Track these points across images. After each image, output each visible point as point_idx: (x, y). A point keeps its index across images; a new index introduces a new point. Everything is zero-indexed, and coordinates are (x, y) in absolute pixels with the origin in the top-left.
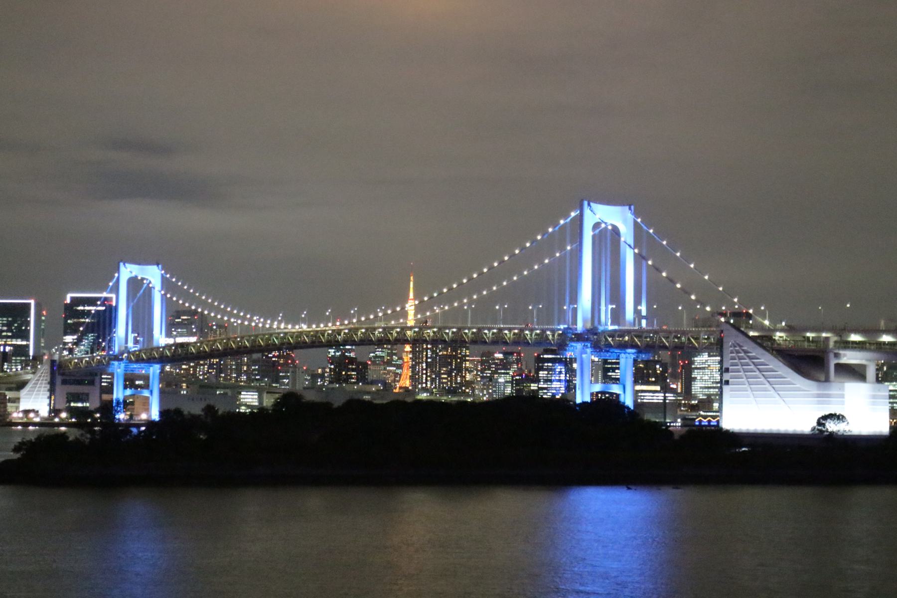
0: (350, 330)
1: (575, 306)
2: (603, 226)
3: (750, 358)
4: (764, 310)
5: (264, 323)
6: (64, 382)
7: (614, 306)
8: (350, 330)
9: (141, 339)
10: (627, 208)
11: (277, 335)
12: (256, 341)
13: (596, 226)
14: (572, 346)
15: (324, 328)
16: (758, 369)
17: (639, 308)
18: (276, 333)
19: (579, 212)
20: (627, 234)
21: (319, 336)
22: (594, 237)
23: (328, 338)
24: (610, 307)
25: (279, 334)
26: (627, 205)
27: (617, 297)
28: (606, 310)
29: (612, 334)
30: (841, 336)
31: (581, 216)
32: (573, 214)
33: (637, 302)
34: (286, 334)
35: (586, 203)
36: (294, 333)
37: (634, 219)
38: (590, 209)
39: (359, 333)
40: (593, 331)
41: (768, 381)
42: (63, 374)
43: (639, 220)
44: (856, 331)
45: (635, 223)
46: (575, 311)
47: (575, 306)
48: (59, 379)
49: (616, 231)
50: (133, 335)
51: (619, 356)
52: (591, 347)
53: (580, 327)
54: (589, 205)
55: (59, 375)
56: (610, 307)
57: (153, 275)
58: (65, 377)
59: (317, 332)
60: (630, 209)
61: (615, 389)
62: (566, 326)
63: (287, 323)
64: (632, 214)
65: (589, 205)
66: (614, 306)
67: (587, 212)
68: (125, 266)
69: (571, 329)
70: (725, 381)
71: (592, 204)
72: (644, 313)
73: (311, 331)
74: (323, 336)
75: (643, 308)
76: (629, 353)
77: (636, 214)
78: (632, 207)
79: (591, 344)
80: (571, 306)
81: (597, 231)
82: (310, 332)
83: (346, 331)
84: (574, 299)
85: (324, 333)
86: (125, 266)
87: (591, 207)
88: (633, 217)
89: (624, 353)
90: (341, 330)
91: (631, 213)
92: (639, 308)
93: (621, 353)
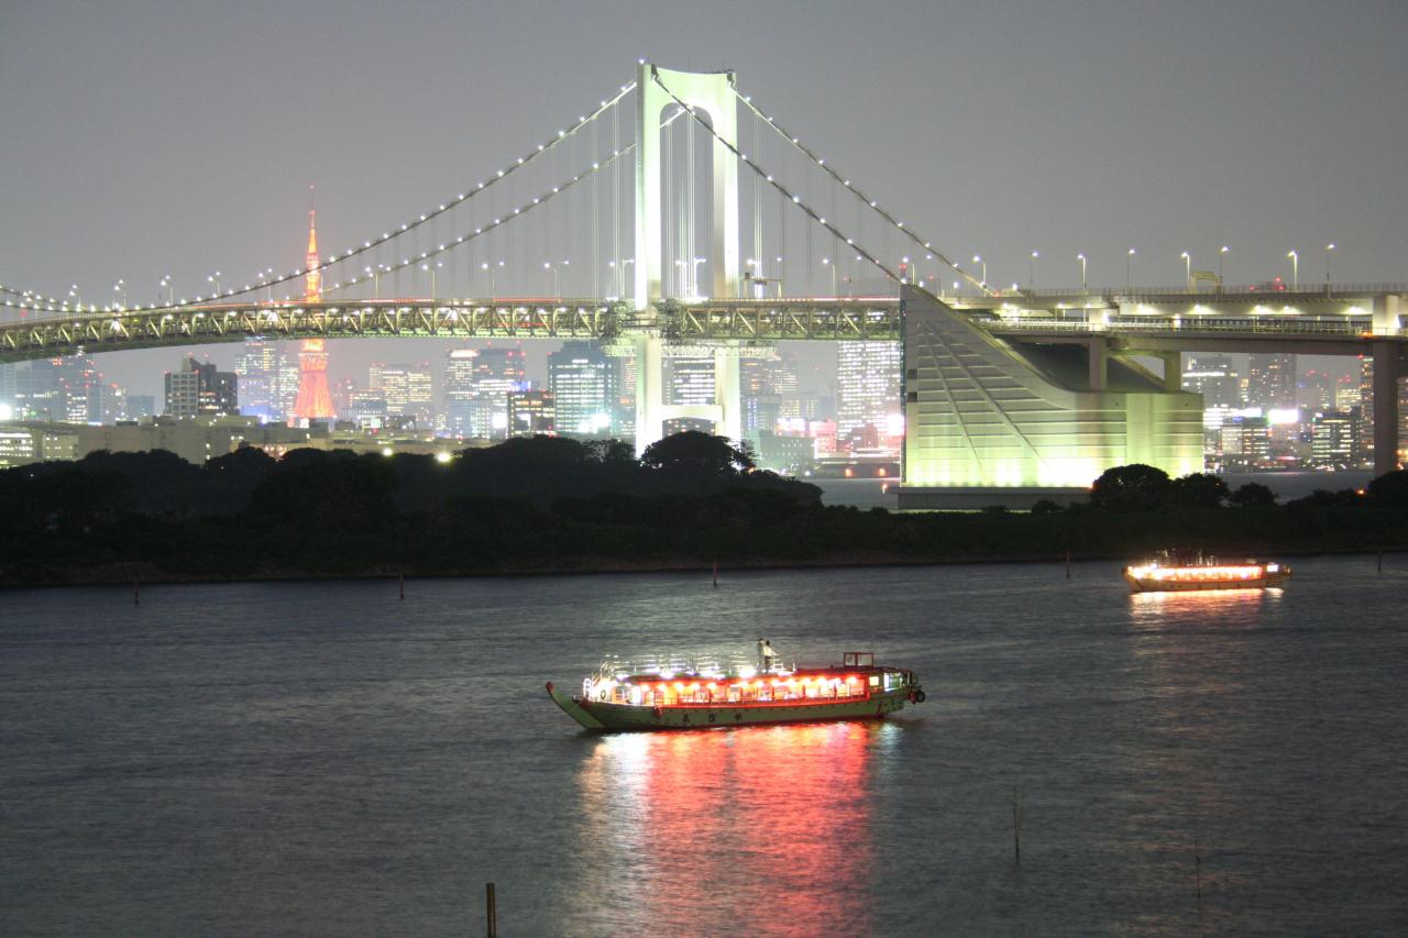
0: (208, 313)
1: (632, 261)
2: (681, 111)
3: (955, 351)
4: (979, 263)
5: (45, 301)
7: (704, 261)
8: (208, 313)
10: (725, 75)
11: (68, 325)
12: (28, 338)
13: (667, 111)
14: (627, 335)
15: (157, 311)
16: (970, 371)
17: (750, 262)
18: (66, 321)
19: (635, 85)
20: (726, 126)
21: (150, 326)
22: (663, 131)
23: (167, 329)
24: (696, 262)
25: (72, 322)
26: (725, 72)
27: (710, 246)
28: (689, 266)
29: (700, 312)
30: (1115, 306)
31: (640, 91)
32: (625, 90)
33: (746, 249)
34: (86, 322)
35: (648, 69)
36: (101, 320)
37: (737, 97)
38: (656, 79)
39: (226, 319)
41: (989, 394)
43: (747, 100)
44: (1148, 298)
45: (740, 103)
46: (630, 269)
47: (632, 261)
49: (704, 123)
51: (713, 352)
52: (661, 337)
53: (640, 302)
54: (654, 71)
56: (696, 262)
59: (145, 318)
60: (730, 78)
62: (616, 299)
63: (86, 303)
65: (654, 71)
66: (704, 261)
67: (650, 85)
69: (624, 304)
70: (910, 394)
71: (659, 70)
72: (758, 274)
73: (136, 316)
74: (158, 325)
75: (757, 264)
76: (732, 347)
77: (741, 88)
78: (734, 75)
79: (663, 331)
80: (625, 262)
81: (669, 122)
82: (130, 317)
83: (201, 315)
84: (629, 250)
85: (159, 320)
87: (657, 75)
88: (736, 93)
89: (724, 347)
90: (191, 314)
92: (750, 262)
93: (716, 347)
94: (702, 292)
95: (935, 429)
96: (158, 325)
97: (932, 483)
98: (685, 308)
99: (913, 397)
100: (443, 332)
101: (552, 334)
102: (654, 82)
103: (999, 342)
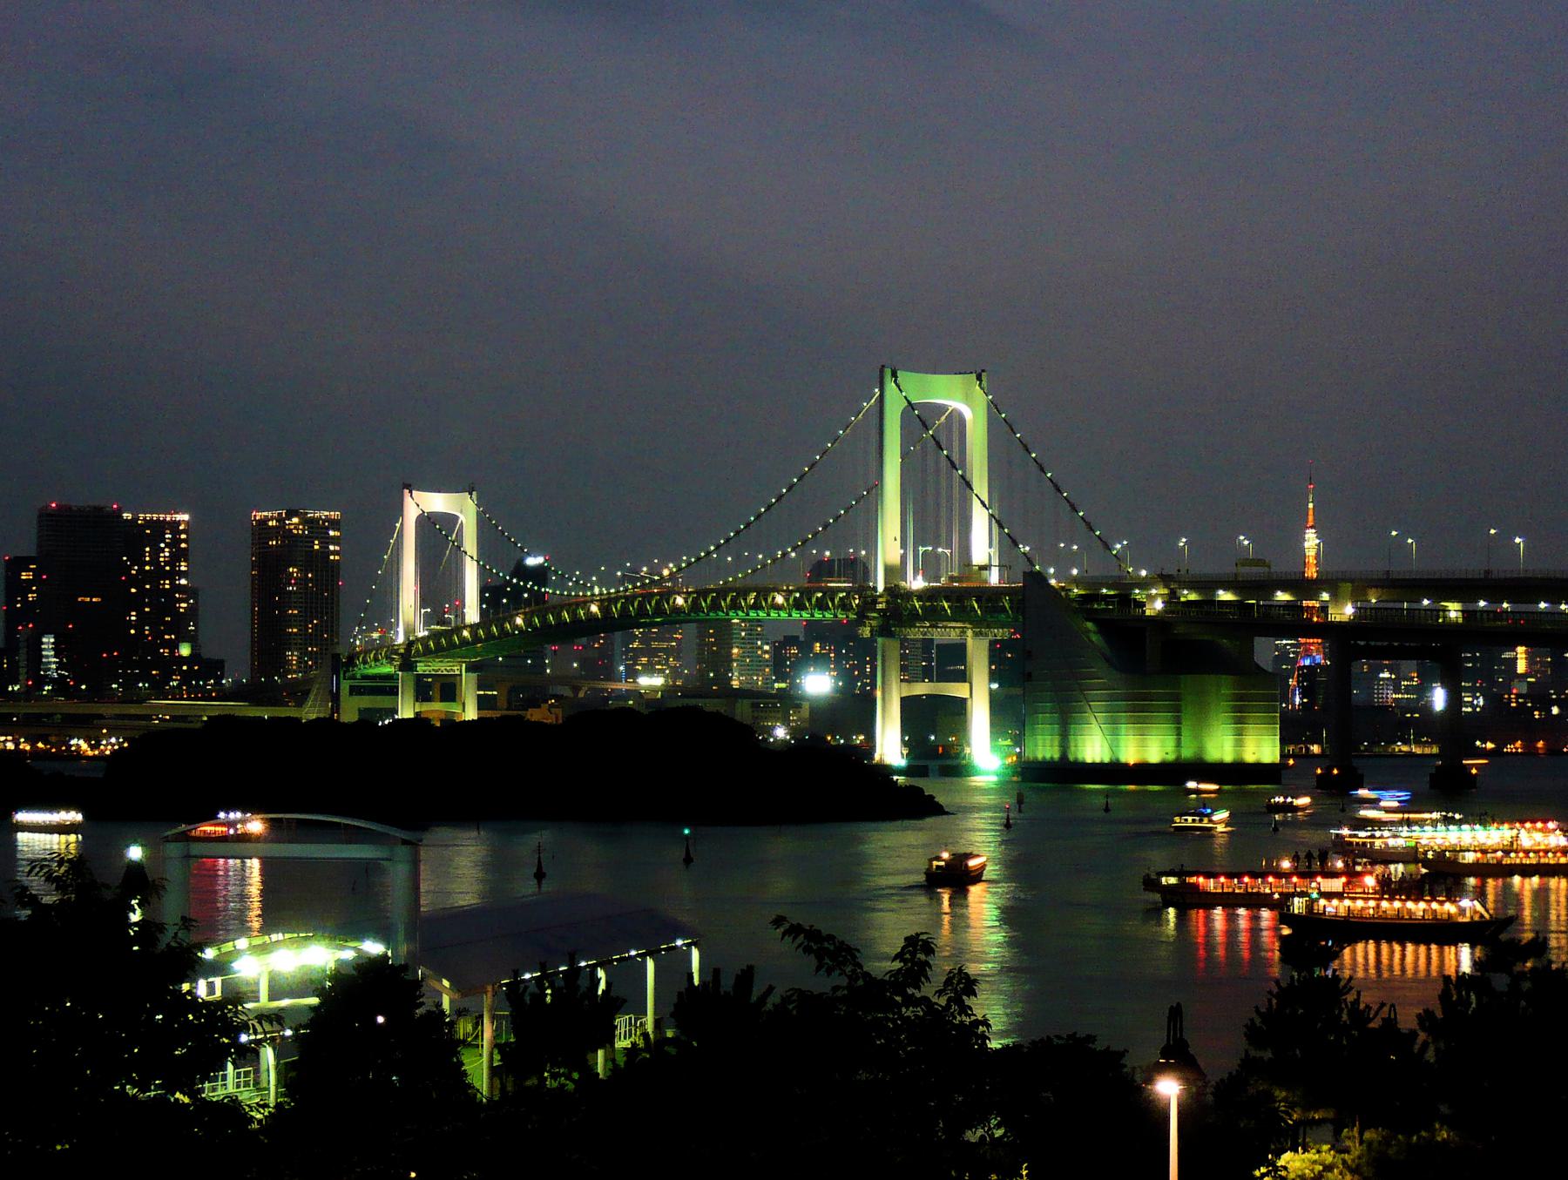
6: (355, 691)
9: (452, 617)
24: (921, 549)
35: (888, 372)
38: (895, 382)
40: (893, 591)
42: (353, 678)
48: (345, 686)
50: (423, 611)
54: (894, 375)
55: (344, 679)
56: (921, 549)
57: (462, 508)
58: (356, 683)
60: (979, 378)
61: (958, 690)
64: (981, 388)
67: (890, 386)
68: (411, 492)
71: (899, 373)
86: (411, 492)
91: (980, 385)
94: (925, 578)
95: (1042, 706)
96: (616, 608)
97: (1040, 756)
98: (909, 595)
99: (1029, 677)
100: (773, 614)
101: (836, 616)
102: (893, 384)
103: (1090, 625)
